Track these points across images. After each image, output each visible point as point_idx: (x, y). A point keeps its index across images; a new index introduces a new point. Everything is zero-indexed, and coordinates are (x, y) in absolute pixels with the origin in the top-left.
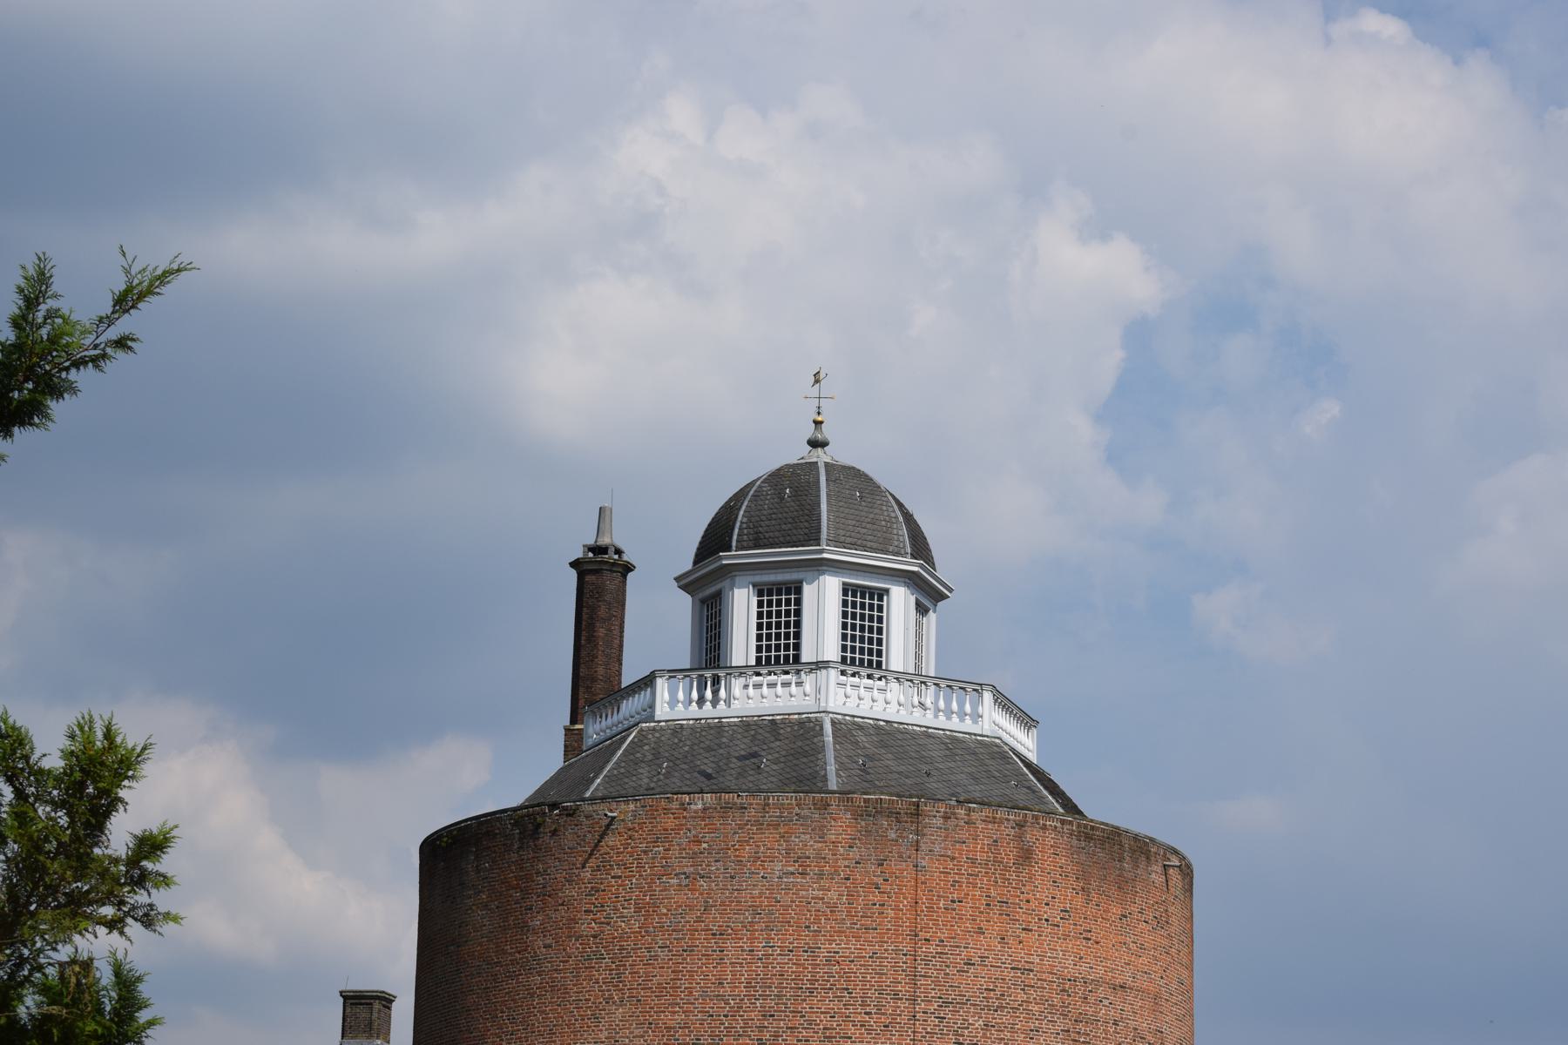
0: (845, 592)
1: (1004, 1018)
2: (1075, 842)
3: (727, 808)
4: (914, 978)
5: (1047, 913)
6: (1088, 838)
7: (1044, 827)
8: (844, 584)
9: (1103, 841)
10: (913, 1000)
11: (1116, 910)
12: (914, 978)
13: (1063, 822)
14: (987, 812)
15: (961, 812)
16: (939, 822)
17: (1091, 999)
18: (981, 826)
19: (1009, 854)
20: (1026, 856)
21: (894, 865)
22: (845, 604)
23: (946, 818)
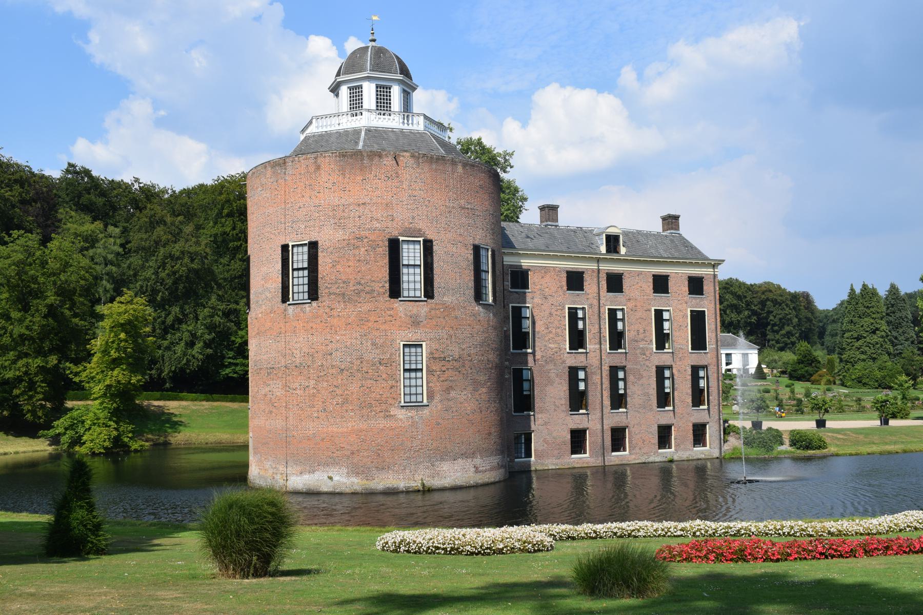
0: (377, 87)
1: (311, 223)
2: (338, 159)
6: (344, 156)
7: (325, 157)
8: (348, 87)
9: (351, 156)
11: (359, 178)
13: (332, 153)
14: (304, 156)
15: (296, 159)
16: (290, 164)
17: (347, 210)
18: (302, 161)
19: (311, 169)
20: (318, 168)
21: (280, 181)
22: (377, 91)
23: (292, 162)
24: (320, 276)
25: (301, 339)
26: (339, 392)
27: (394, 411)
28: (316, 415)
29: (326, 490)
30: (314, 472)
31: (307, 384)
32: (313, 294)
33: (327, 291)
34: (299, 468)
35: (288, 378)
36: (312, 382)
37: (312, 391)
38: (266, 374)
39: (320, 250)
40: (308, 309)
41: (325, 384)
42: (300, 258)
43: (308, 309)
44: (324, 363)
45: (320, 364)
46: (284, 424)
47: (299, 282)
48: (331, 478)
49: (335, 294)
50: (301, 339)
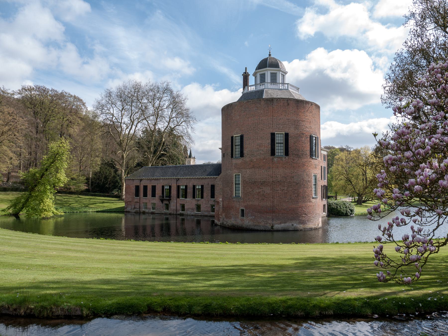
1: (285, 126)
3: (248, 102)
4: (273, 121)
5: (291, 112)
10: (273, 124)
12: (273, 121)
19: (286, 104)
20: (288, 104)
24: (289, 147)
25: (281, 171)
26: (296, 192)
27: (312, 200)
28: (287, 200)
29: (291, 229)
30: (286, 223)
31: (283, 188)
32: (287, 153)
33: (292, 153)
34: (279, 222)
35: (274, 186)
36: (286, 188)
37: (286, 191)
38: (260, 184)
39: (289, 137)
40: (284, 159)
41: (291, 189)
42: (279, 139)
43: (284, 159)
44: (291, 181)
45: (289, 181)
46: (272, 204)
47: (280, 149)
48: (293, 225)
49: (295, 154)
50: (281, 171)
